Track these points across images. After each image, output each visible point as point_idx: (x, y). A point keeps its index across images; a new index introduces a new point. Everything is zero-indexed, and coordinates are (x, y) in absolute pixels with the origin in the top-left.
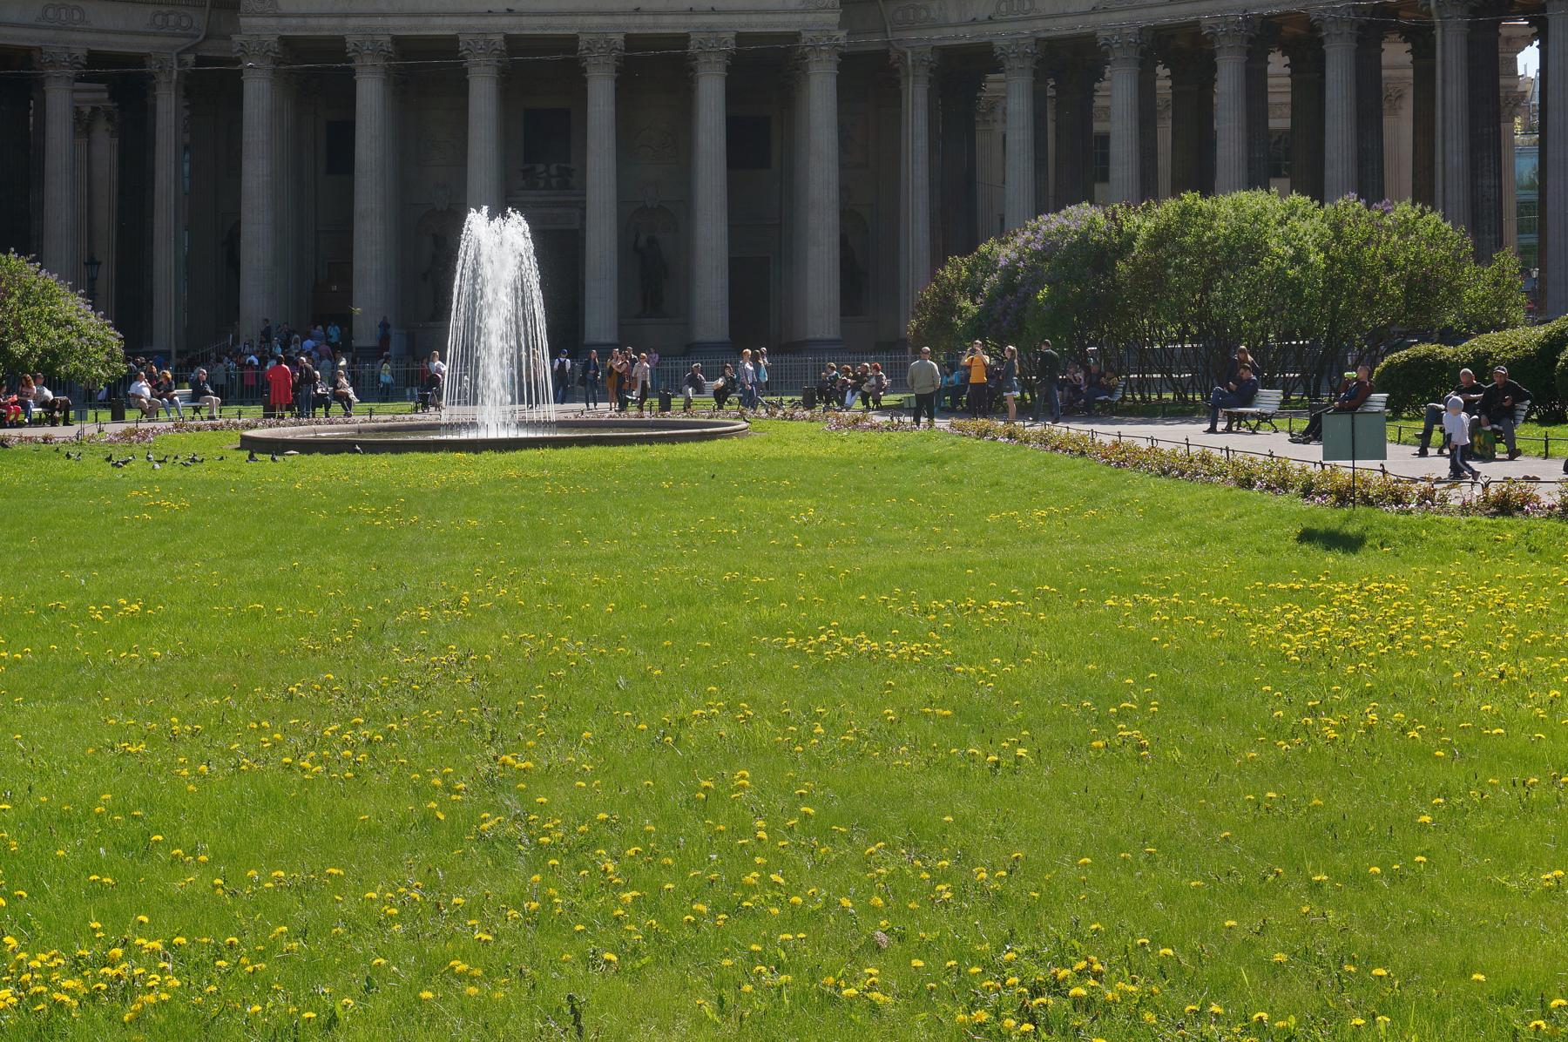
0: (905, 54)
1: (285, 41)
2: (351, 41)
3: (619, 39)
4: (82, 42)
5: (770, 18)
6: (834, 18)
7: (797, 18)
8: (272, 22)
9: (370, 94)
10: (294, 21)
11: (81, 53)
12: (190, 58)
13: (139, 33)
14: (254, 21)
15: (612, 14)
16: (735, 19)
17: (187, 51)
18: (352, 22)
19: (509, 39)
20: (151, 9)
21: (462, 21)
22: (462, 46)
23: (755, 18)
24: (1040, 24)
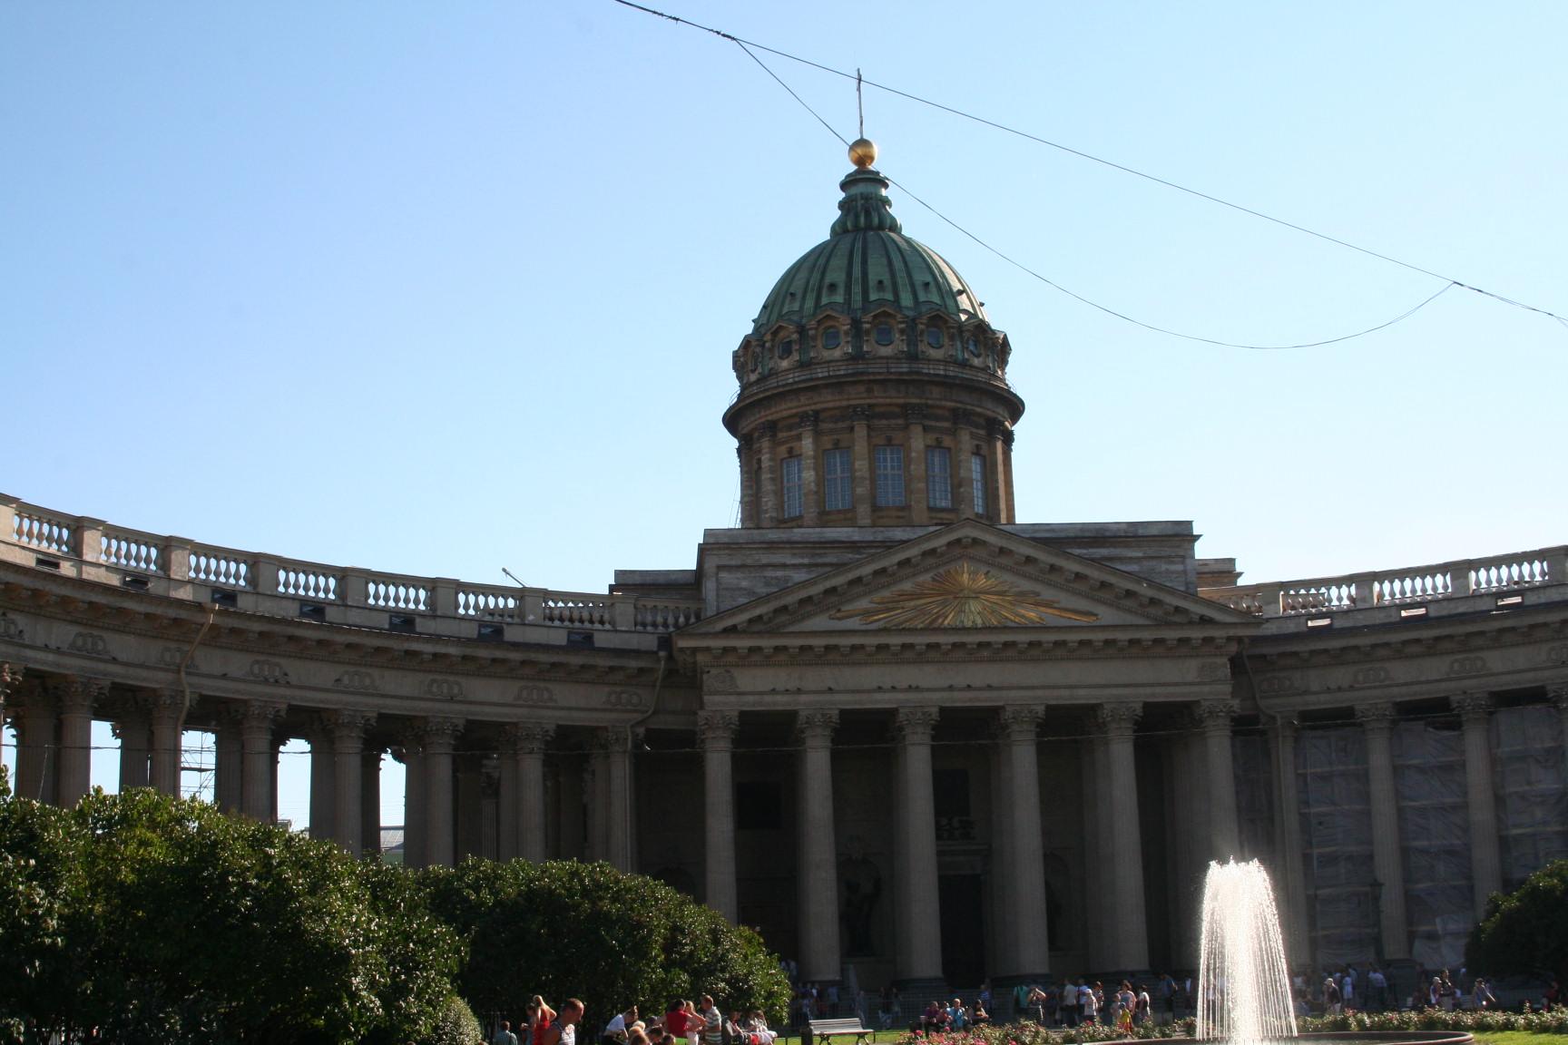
0: (1274, 718)
1: (742, 714)
2: (803, 714)
3: (1041, 710)
4: (551, 719)
5: (1171, 689)
6: (1228, 688)
7: (1195, 689)
8: (733, 698)
9: (817, 763)
10: (751, 698)
11: (551, 727)
12: (641, 730)
13: (596, 710)
14: (717, 698)
15: (1033, 688)
16: (1141, 691)
17: (639, 723)
18: (803, 698)
19: (942, 710)
20: (607, 689)
22: (901, 717)
23: (1158, 690)
24: (1396, 690)
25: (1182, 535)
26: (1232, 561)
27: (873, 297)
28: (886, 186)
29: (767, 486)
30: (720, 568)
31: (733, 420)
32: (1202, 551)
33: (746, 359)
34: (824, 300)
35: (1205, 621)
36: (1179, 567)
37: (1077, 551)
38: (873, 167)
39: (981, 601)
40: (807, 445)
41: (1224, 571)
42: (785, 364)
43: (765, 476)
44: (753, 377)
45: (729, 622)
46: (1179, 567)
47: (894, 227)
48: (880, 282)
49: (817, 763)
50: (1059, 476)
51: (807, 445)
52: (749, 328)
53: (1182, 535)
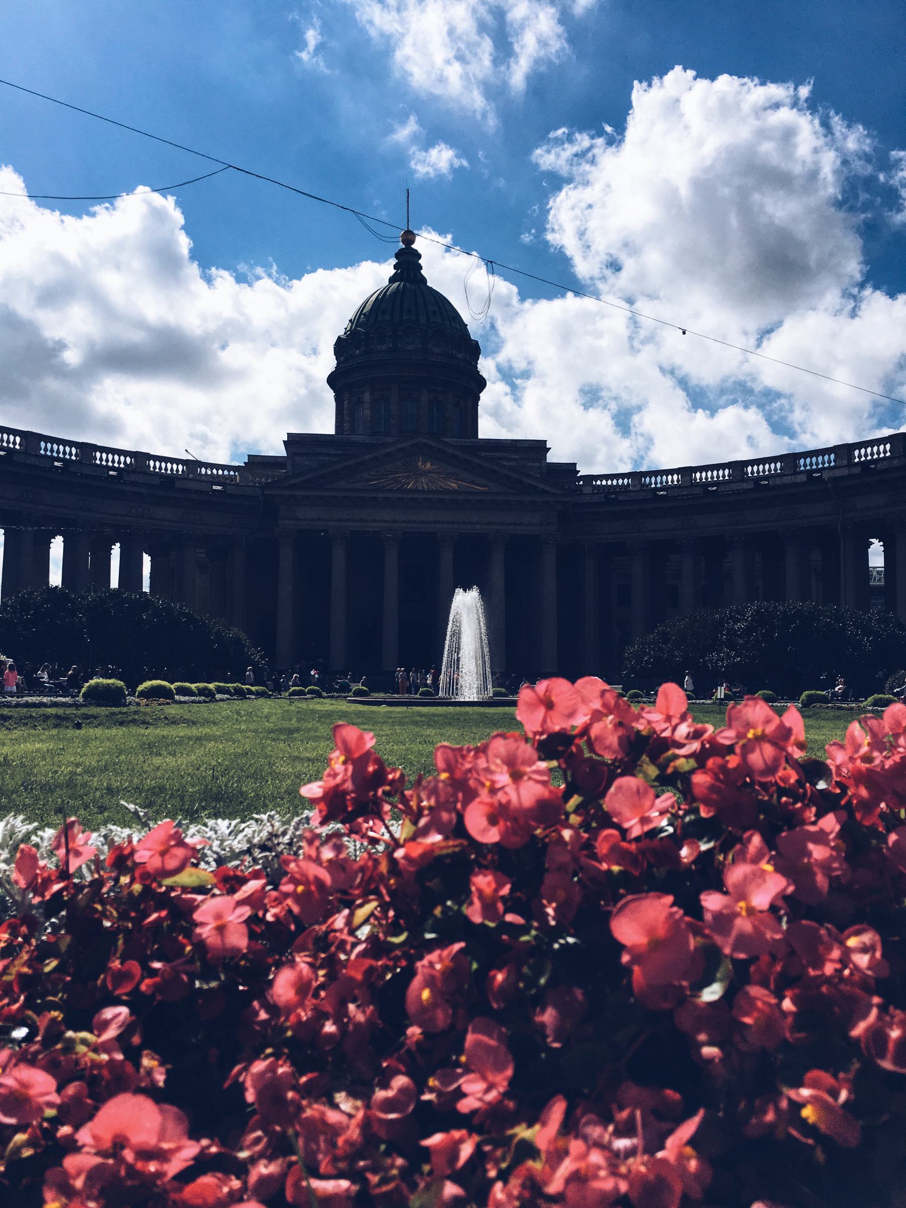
9: (339, 555)
21: (384, 525)
25: (541, 447)
26: (575, 464)
27: (405, 318)
28: (419, 256)
29: (347, 418)
30: (295, 454)
31: (332, 380)
32: (551, 458)
33: (341, 347)
34: (379, 319)
35: (544, 492)
36: (537, 465)
37: (484, 454)
38: (414, 246)
39: (428, 477)
40: (367, 396)
41: (570, 469)
42: (357, 352)
43: (345, 412)
44: (342, 359)
45: (292, 482)
46: (537, 465)
47: (424, 280)
48: (410, 310)
49: (339, 555)
50: (499, 417)
51: (367, 396)
52: (341, 332)
53: (541, 447)
